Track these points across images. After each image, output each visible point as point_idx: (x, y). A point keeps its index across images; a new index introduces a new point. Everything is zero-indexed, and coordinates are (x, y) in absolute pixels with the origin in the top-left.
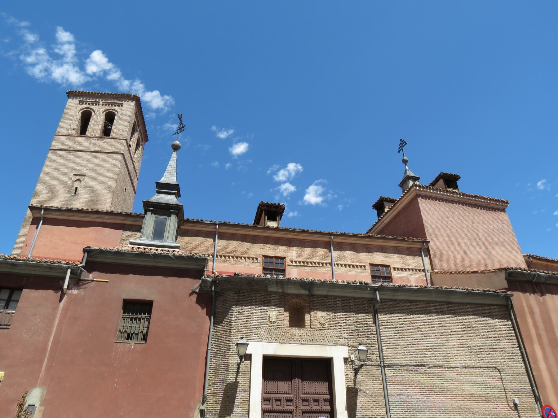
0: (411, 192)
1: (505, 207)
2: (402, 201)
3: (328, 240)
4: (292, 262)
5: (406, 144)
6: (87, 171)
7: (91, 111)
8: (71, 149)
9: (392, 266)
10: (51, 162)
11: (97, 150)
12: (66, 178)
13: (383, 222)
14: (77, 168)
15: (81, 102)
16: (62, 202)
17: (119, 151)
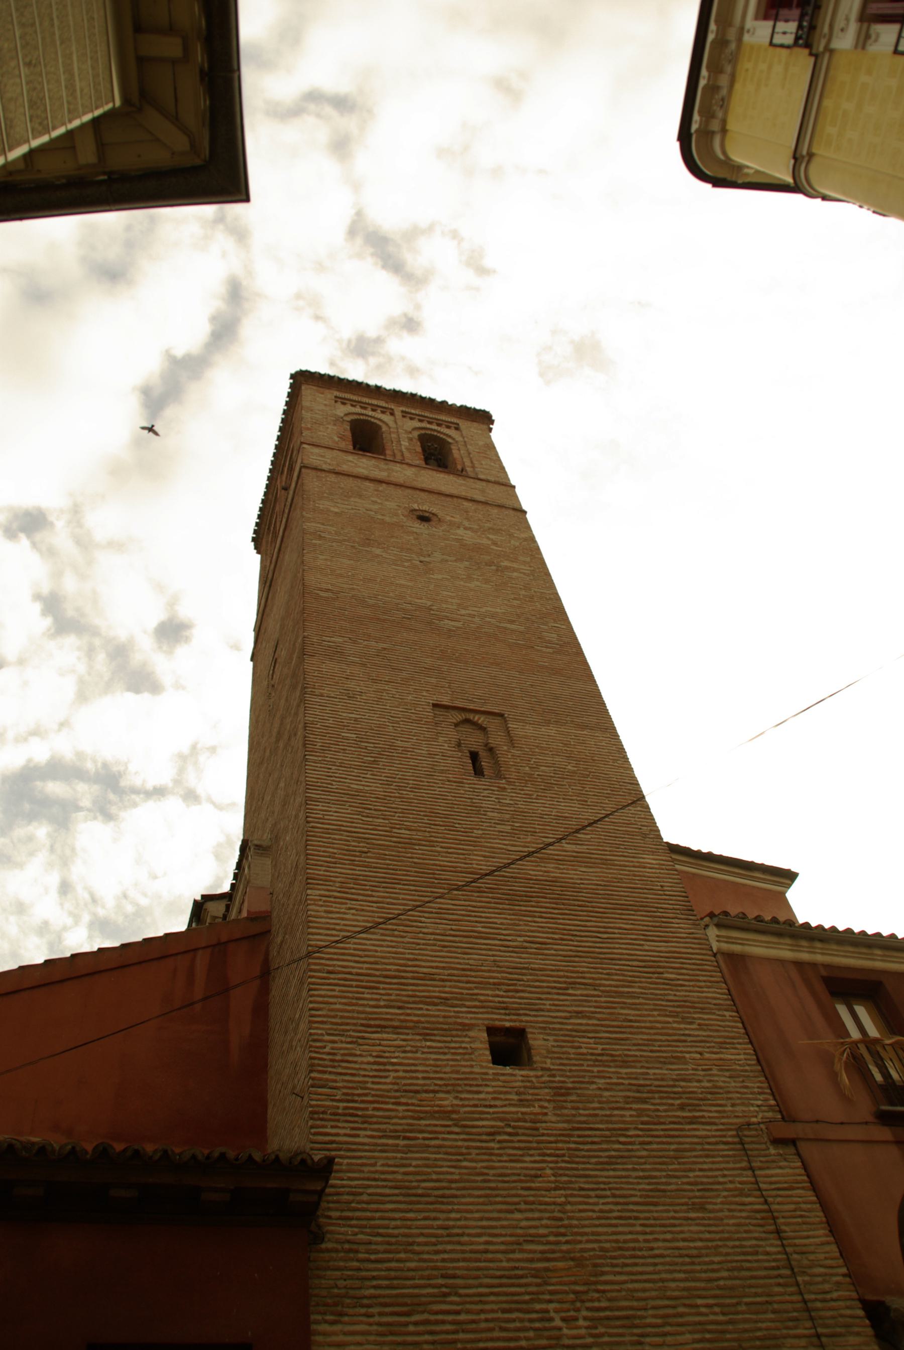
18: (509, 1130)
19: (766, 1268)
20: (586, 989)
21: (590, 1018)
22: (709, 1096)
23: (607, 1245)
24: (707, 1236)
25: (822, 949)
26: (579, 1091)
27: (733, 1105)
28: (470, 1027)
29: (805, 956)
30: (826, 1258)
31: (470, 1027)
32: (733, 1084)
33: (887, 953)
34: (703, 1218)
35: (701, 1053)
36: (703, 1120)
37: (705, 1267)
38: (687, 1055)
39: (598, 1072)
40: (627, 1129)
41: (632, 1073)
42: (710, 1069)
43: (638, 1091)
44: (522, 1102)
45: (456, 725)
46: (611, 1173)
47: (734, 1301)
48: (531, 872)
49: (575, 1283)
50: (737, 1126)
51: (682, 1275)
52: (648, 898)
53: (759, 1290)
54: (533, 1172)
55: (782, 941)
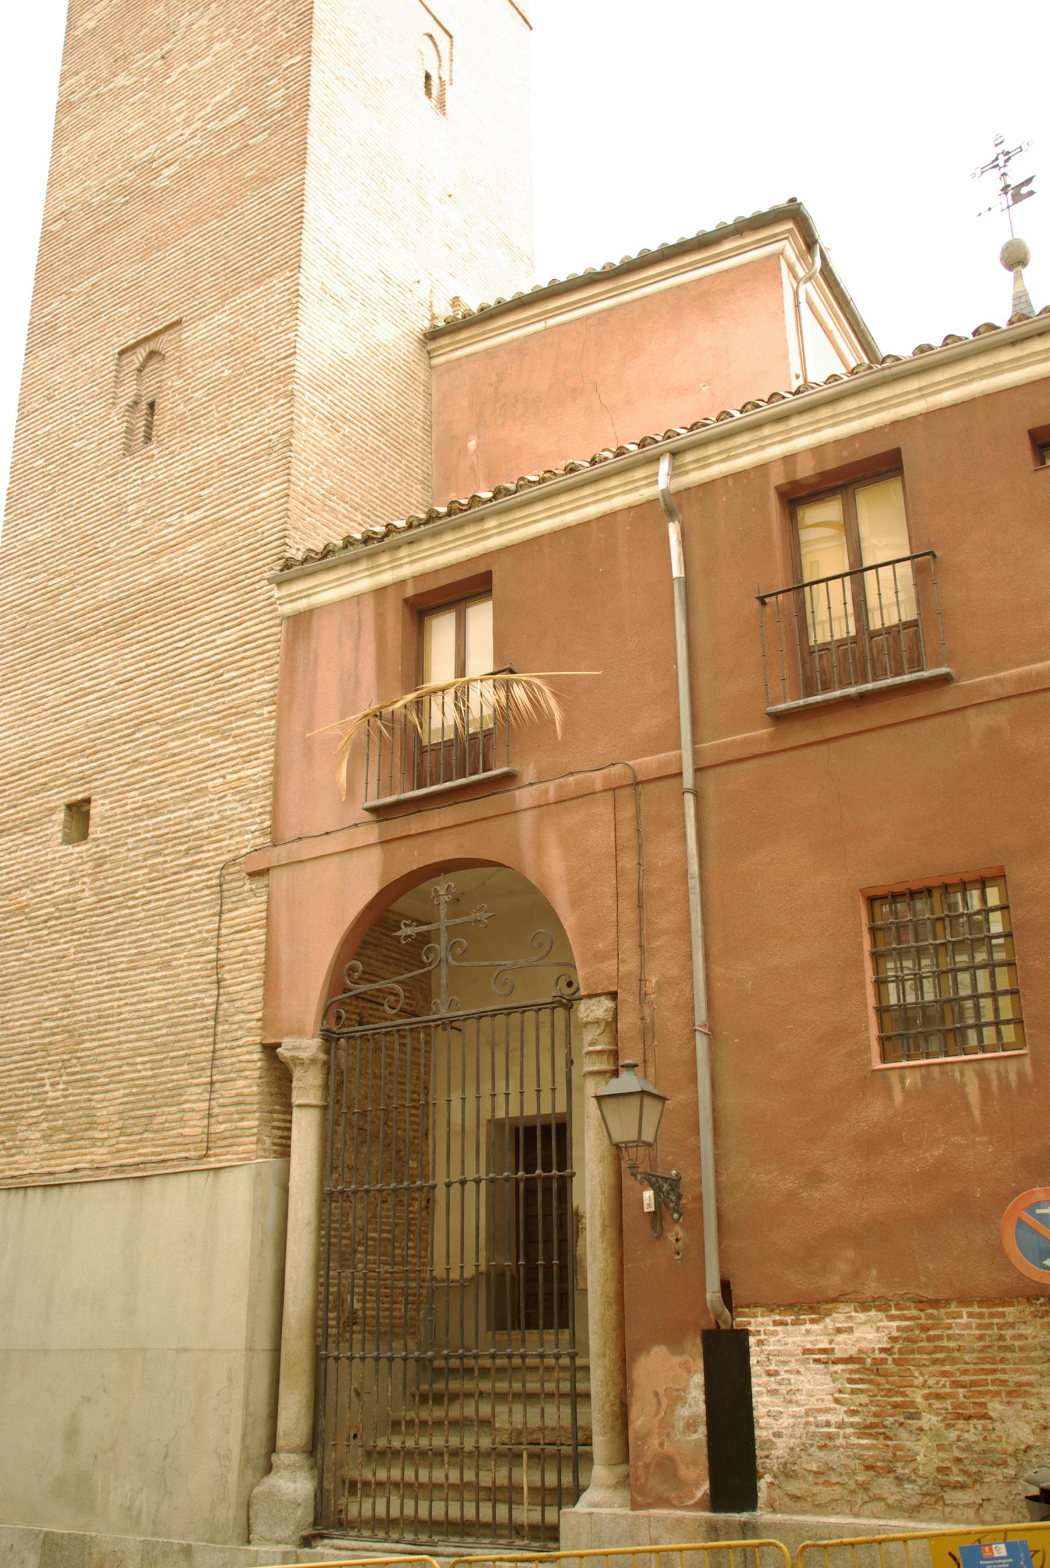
18: (57, 914)
19: (198, 1021)
20: (150, 726)
21: (142, 764)
22: (213, 832)
23: (91, 1015)
24: (164, 994)
25: (409, 556)
26: (112, 858)
27: (231, 838)
28: (52, 810)
29: (387, 577)
30: (249, 1004)
31: (52, 810)
32: (241, 809)
33: (505, 519)
34: (165, 977)
35: (224, 777)
36: (199, 864)
37: (152, 1026)
38: (210, 784)
39: (133, 829)
40: (136, 891)
41: (157, 823)
42: (225, 796)
43: (157, 843)
44: (73, 882)
46: (113, 942)
47: (162, 1056)
48: (144, 580)
49: (64, 1053)
50: (221, 866)
51: (134, 1036)
52: (241, 562)
53: (185, 1044)
54: (61, 954)
55: (355, 569)
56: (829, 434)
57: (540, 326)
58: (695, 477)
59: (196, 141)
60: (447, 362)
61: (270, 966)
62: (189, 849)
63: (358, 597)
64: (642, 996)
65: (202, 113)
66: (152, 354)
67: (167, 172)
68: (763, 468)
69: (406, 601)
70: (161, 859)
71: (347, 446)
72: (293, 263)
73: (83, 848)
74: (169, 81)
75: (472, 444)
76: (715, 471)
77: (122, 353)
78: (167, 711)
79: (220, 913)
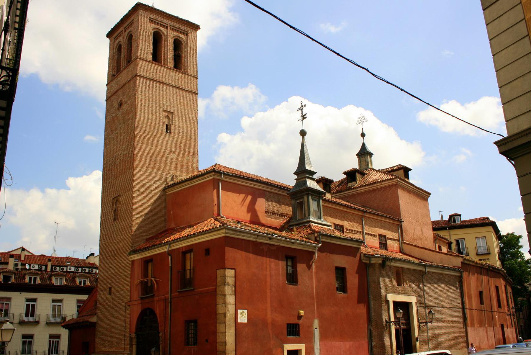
0: (393, 181)
1: (428, 197)
2: (382, 183)
3: (361, 214)
4: (346, 229)
5: (367, 121)
6: (174, 109)
7: (159, 32)
8: (155, 78)
9: (387, 237)
10: (141, 92)
11: (177, 85)
12: (158, 112)
13: (357, 190)
14: (165, 103)
15: (152, 21)
16: (160, 140)
17: (195, 91)
29: (142, 257)
45: (116, 203)
56: (186, 244)
57: (181, 189)
58: (173, 248)
59: (121, 155)
60: (169, 194)
61: (130, 321)
62: (122, 299)
63: (139, 259)
64: (164, 333)
65: (122, 149)
66: (117, 200)
67: (118, 161)
68: (180, 248)
69: (144, 261)
70: (119, 300)
71: (145, 221)
72: (132, 189)
73: (111, 296)
74: (118, 139)
75: (172, 212)
76: (175, 247)
77: (113, 199)
78: (120, 274)
79: (125, 311)
